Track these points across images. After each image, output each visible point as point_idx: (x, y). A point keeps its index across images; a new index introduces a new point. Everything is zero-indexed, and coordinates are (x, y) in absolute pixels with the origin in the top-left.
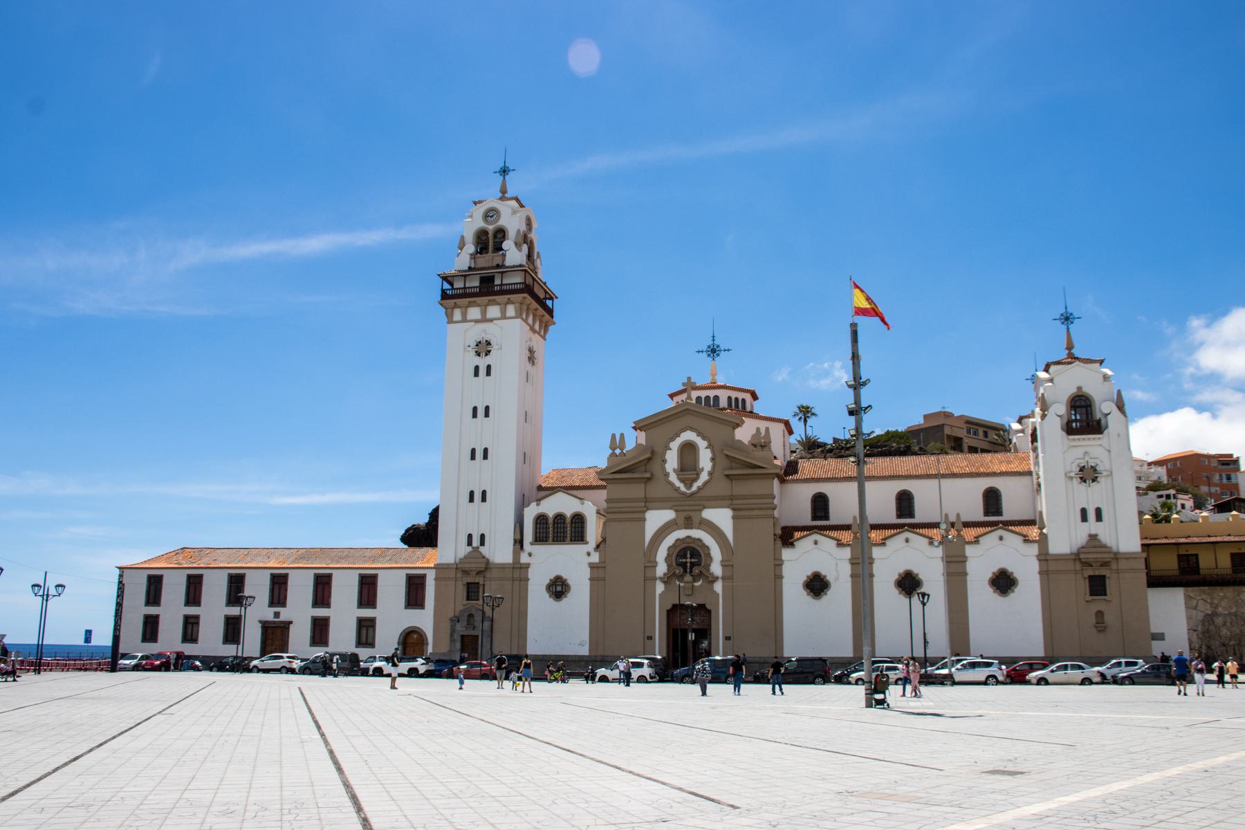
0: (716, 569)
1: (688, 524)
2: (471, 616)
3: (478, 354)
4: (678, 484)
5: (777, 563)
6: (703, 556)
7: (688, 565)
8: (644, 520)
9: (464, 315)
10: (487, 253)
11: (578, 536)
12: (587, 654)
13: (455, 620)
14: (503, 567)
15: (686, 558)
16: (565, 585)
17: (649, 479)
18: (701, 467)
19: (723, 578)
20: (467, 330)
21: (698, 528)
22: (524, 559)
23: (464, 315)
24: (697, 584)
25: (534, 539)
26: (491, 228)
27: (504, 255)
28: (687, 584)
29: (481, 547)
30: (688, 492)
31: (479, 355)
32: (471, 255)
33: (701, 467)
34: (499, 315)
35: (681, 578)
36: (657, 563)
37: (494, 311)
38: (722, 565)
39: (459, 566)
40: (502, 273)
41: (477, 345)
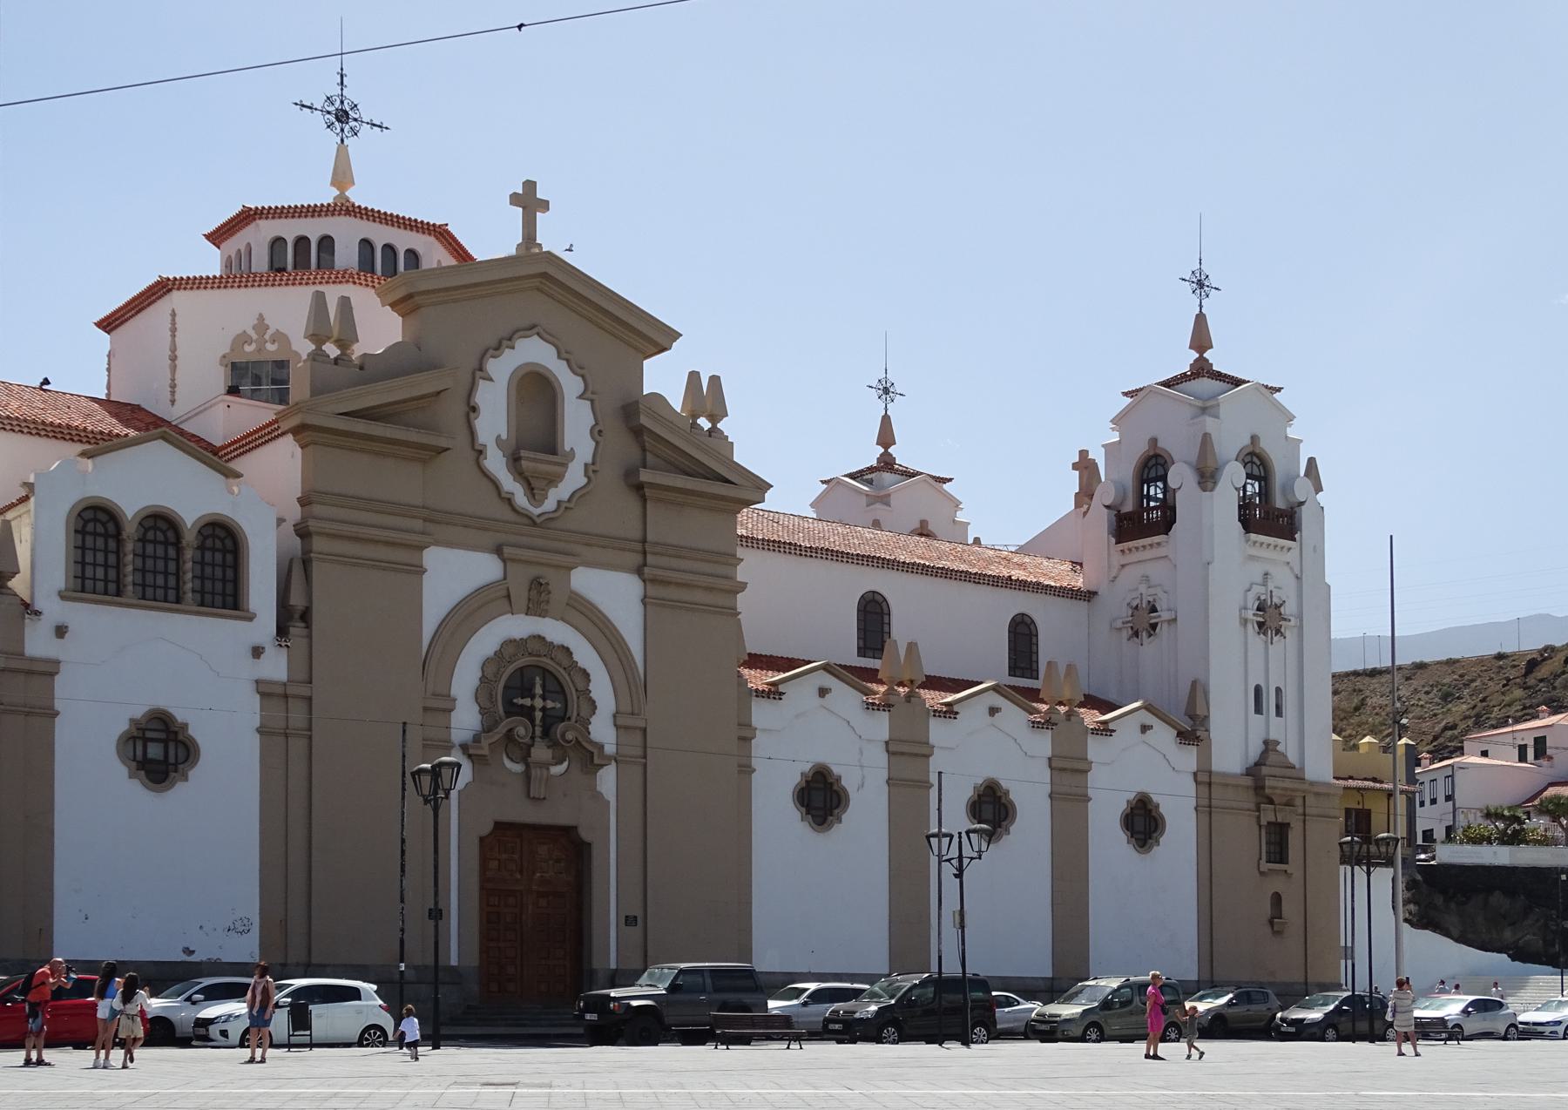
0: (602, 730)
1: (538, 599)
4: (509, 484)
5: (746, 733)
7: (538, 715)
8: (420, 570)
15: (533, 697)
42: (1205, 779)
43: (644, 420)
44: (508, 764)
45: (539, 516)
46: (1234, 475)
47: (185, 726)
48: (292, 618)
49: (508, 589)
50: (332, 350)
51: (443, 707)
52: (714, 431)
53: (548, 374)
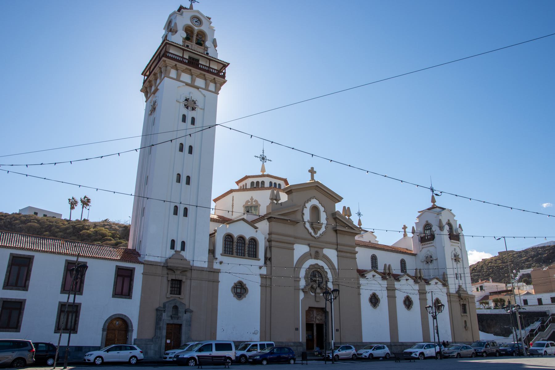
1: (317, 255)
4: (311, 230)
5: (359, 286)
6: (324, 276)
7: (317, 282)
11: (254, 255)
13: (159, 311)
20: (179, 87)
29: (182, 252)
31: (187, 108)
37: (200, 82)
42: (449, 295)
43: (337, 216)
45: (317, 237)
46: (447, 228)
47: (245, 285)
48: (267, 259)
49: (311, 253)
51: (297, 280)
52: (349, 219)
53: (317, 206)
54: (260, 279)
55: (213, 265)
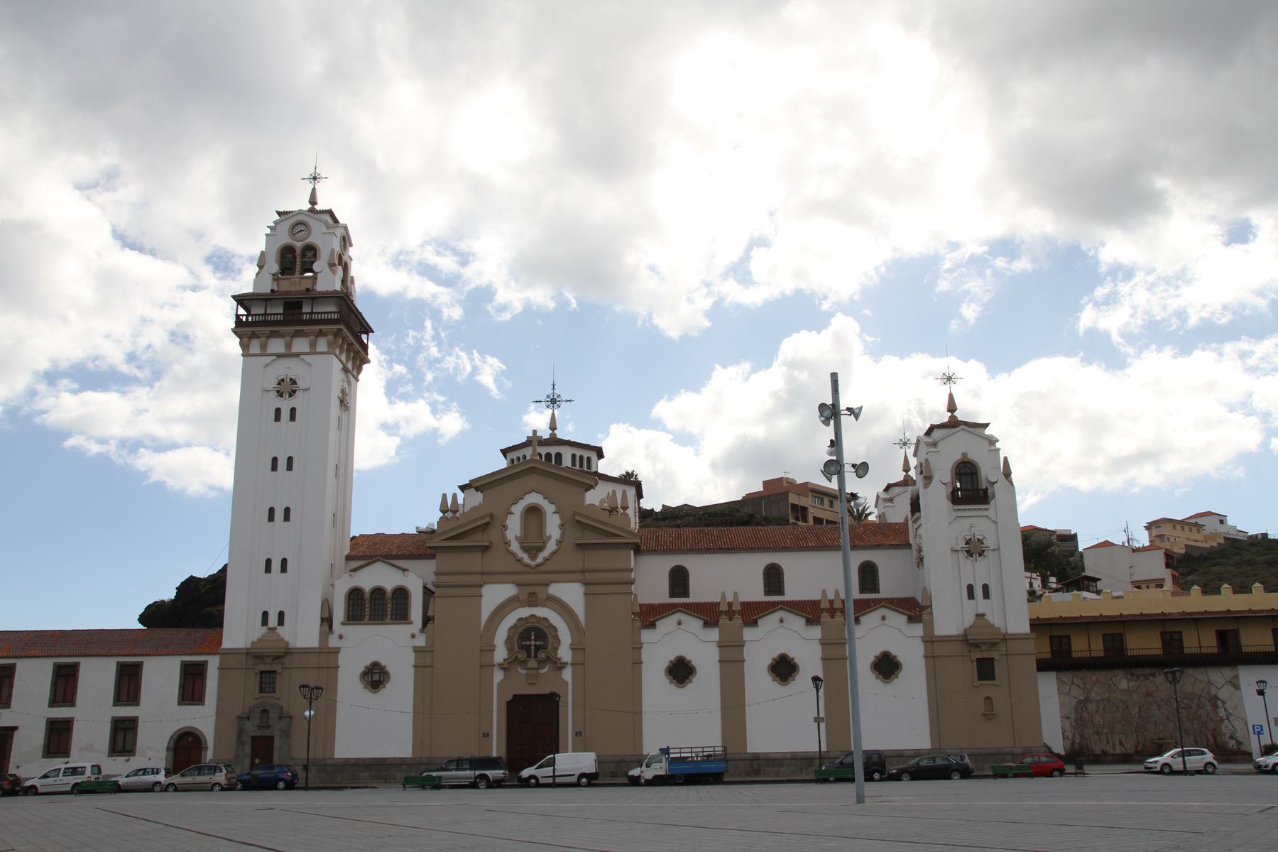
0: (565, 653)
1: (533, 601)
2: (265, 712)
3: (280, 394)
4: (521, 554)
7: (533, 647)
8: (481, 596)
9: (264, 346)
10: (294, 274)
11: (401, 615)
12: (409, 755)
14: (307, 652)
16: (384, 673)
17: (486, 548)
18: (548, 535)
19: (572, 664)
21: (544, 606)
22: (333, 642)
23: (264, 346)
24: (542, 671)
25: (346, 619)
26: (299, 245)
27: (314, 278)
28: (531, 672)
29: (278, 627)
30: (533, 563)
31: (281, 395)
32: (274, 275)
33: (548, 535)
34: (307, 350)
35: (524, 662)
36: (495, 646)
37: (300, 345)
38: (572, 649)
39: (251, 651)
40: (313, 299)
41: (279, 384)
44: (520, 670)
50: (449, 515)
51: (492, 650)
54: (413, 655)
55: (327, 641)
